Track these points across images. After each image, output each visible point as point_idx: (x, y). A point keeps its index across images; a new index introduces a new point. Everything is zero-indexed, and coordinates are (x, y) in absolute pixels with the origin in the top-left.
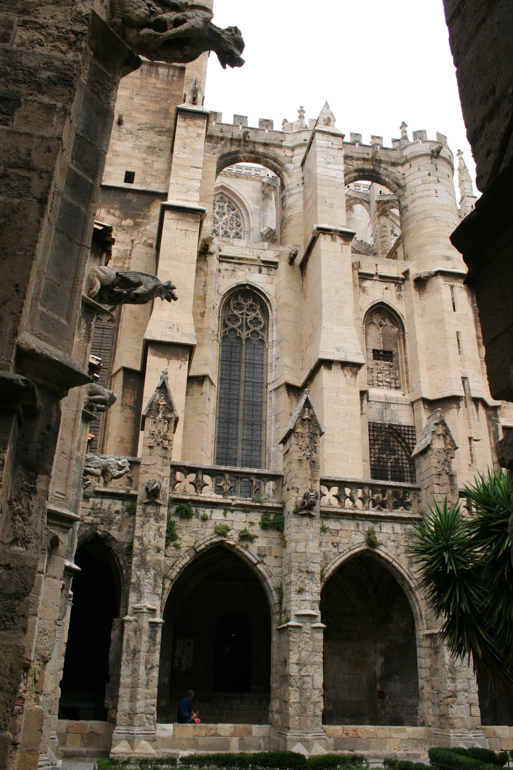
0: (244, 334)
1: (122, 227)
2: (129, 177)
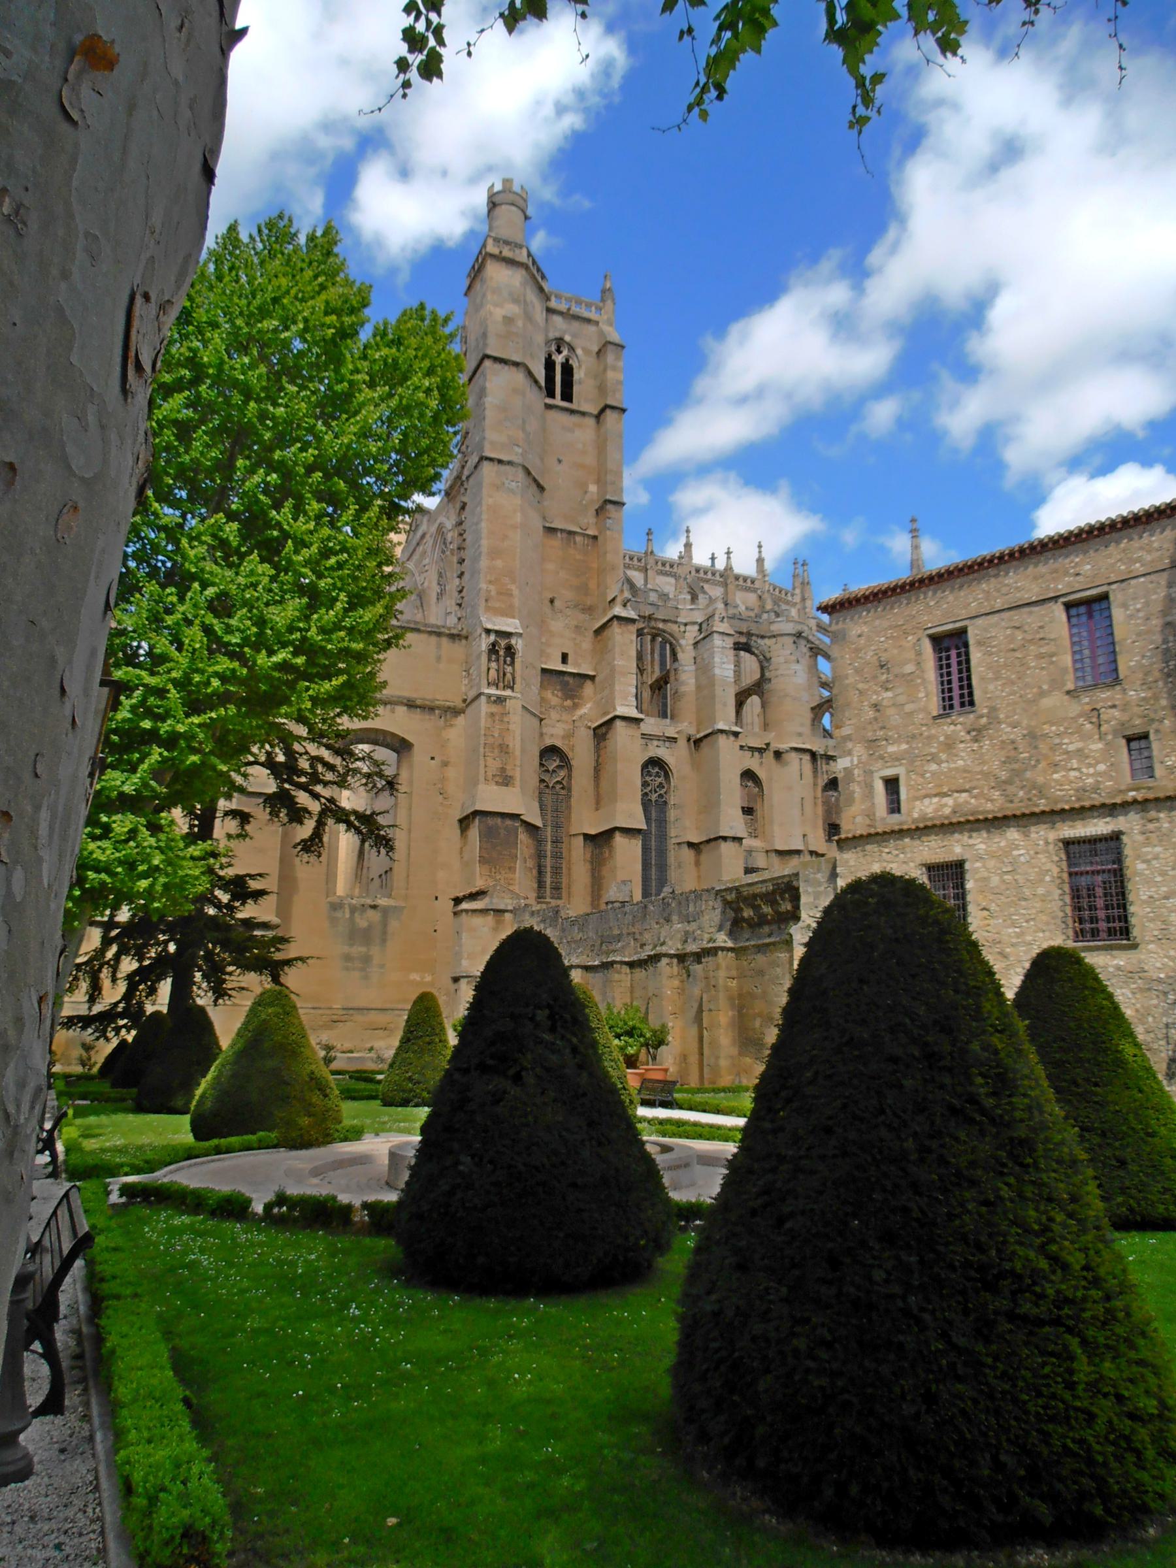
0: (654, 797)
1: (564, 707)
2: (565, 658)
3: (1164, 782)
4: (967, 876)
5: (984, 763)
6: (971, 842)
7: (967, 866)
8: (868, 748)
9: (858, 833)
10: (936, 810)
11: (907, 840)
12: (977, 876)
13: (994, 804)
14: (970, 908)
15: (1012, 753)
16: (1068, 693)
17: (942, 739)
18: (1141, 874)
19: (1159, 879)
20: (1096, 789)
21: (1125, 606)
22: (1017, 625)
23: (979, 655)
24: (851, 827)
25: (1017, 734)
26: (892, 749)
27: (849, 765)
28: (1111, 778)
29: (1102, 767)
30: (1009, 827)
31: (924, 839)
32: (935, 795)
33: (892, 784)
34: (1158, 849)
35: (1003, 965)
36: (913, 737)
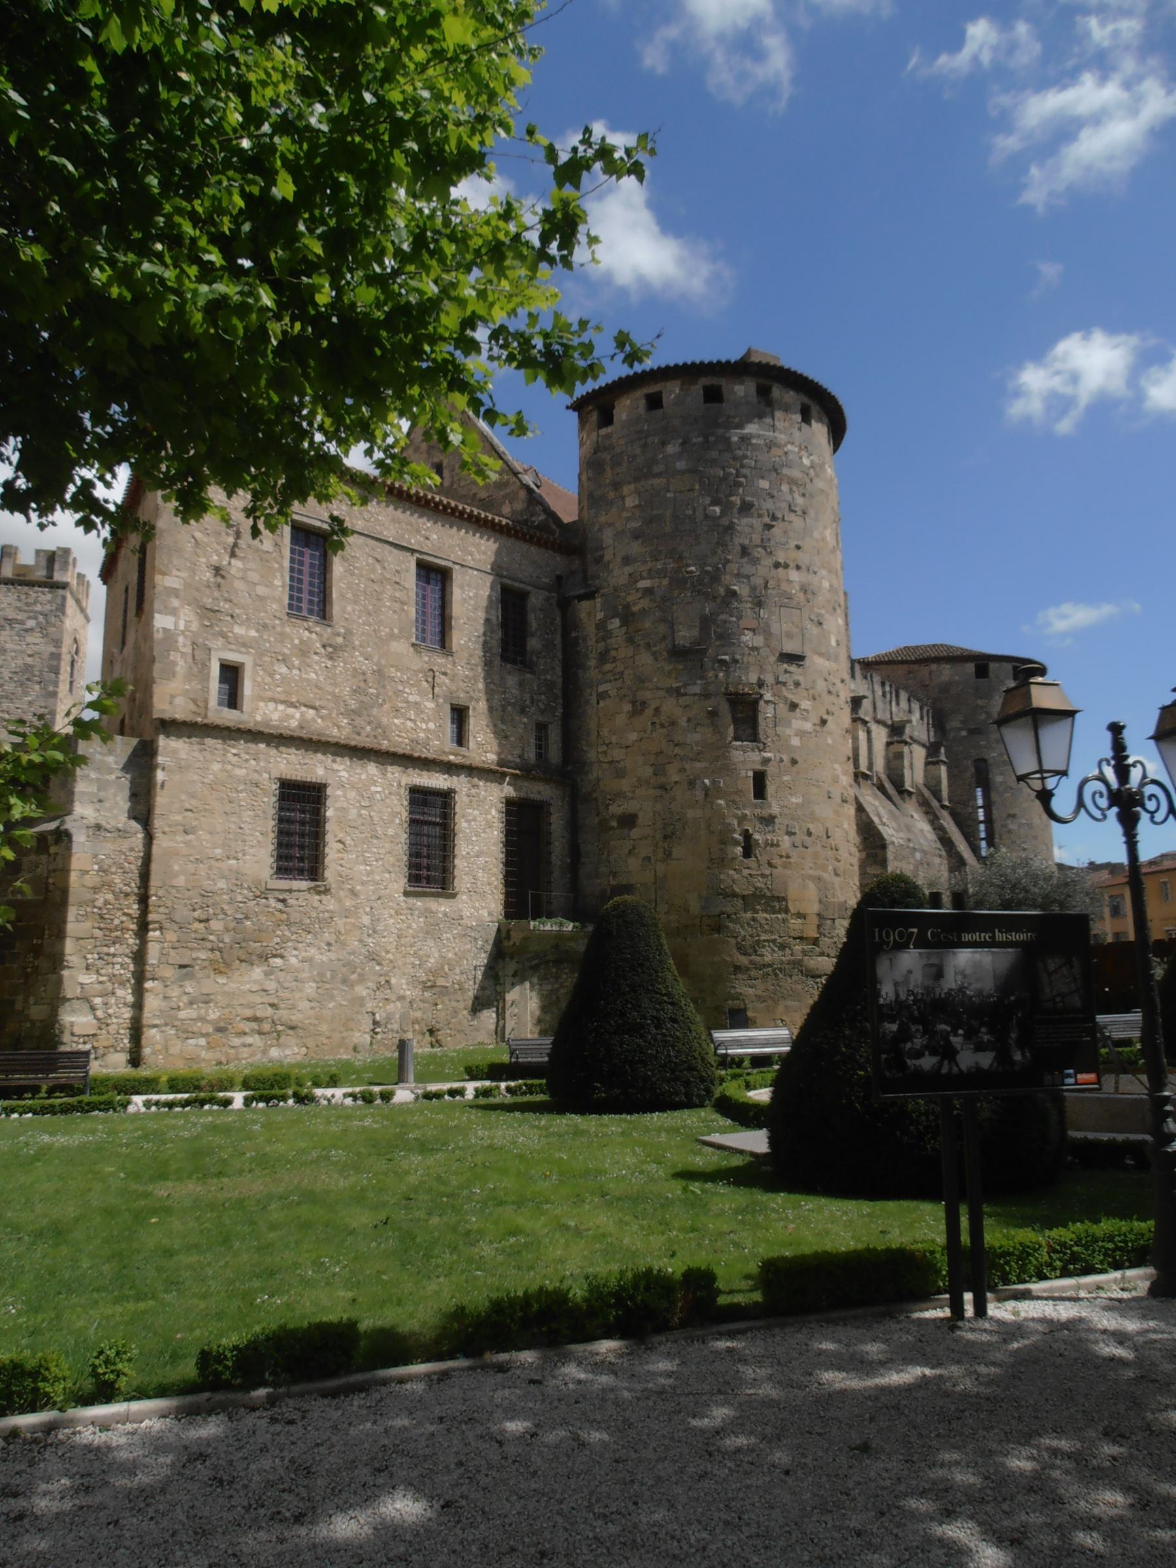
3: (474, 755)
4: (328, 803)
5: (336, 685)
6: (335, 766)
7: (329, 791)
8: (201, 617)
9: (179, 716)
10: (281, 720)
11: (262, 746)
12: (338, 805)
13: (340, 731)
14: (329, 838)
15: (362, 684)
16: (413, 645)
17: (297, 642)
18: (464, 832)
19: (474, 838)
20: (426, 744)
21: (462, 588)
22: (378, 557)
23: (341, 569)
24: (167, 707)
25: (366, 666)
26: (239, 630)
27: (172, 627)
28: (438, 737)
29: (431, 725)
30: (369, 760)
31: (282, 749)
32: (282, 702)
33: (231, 674)
34: (476, 812)
35: (353, 903)
36: (265, 626)
